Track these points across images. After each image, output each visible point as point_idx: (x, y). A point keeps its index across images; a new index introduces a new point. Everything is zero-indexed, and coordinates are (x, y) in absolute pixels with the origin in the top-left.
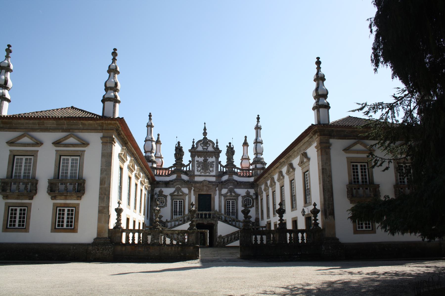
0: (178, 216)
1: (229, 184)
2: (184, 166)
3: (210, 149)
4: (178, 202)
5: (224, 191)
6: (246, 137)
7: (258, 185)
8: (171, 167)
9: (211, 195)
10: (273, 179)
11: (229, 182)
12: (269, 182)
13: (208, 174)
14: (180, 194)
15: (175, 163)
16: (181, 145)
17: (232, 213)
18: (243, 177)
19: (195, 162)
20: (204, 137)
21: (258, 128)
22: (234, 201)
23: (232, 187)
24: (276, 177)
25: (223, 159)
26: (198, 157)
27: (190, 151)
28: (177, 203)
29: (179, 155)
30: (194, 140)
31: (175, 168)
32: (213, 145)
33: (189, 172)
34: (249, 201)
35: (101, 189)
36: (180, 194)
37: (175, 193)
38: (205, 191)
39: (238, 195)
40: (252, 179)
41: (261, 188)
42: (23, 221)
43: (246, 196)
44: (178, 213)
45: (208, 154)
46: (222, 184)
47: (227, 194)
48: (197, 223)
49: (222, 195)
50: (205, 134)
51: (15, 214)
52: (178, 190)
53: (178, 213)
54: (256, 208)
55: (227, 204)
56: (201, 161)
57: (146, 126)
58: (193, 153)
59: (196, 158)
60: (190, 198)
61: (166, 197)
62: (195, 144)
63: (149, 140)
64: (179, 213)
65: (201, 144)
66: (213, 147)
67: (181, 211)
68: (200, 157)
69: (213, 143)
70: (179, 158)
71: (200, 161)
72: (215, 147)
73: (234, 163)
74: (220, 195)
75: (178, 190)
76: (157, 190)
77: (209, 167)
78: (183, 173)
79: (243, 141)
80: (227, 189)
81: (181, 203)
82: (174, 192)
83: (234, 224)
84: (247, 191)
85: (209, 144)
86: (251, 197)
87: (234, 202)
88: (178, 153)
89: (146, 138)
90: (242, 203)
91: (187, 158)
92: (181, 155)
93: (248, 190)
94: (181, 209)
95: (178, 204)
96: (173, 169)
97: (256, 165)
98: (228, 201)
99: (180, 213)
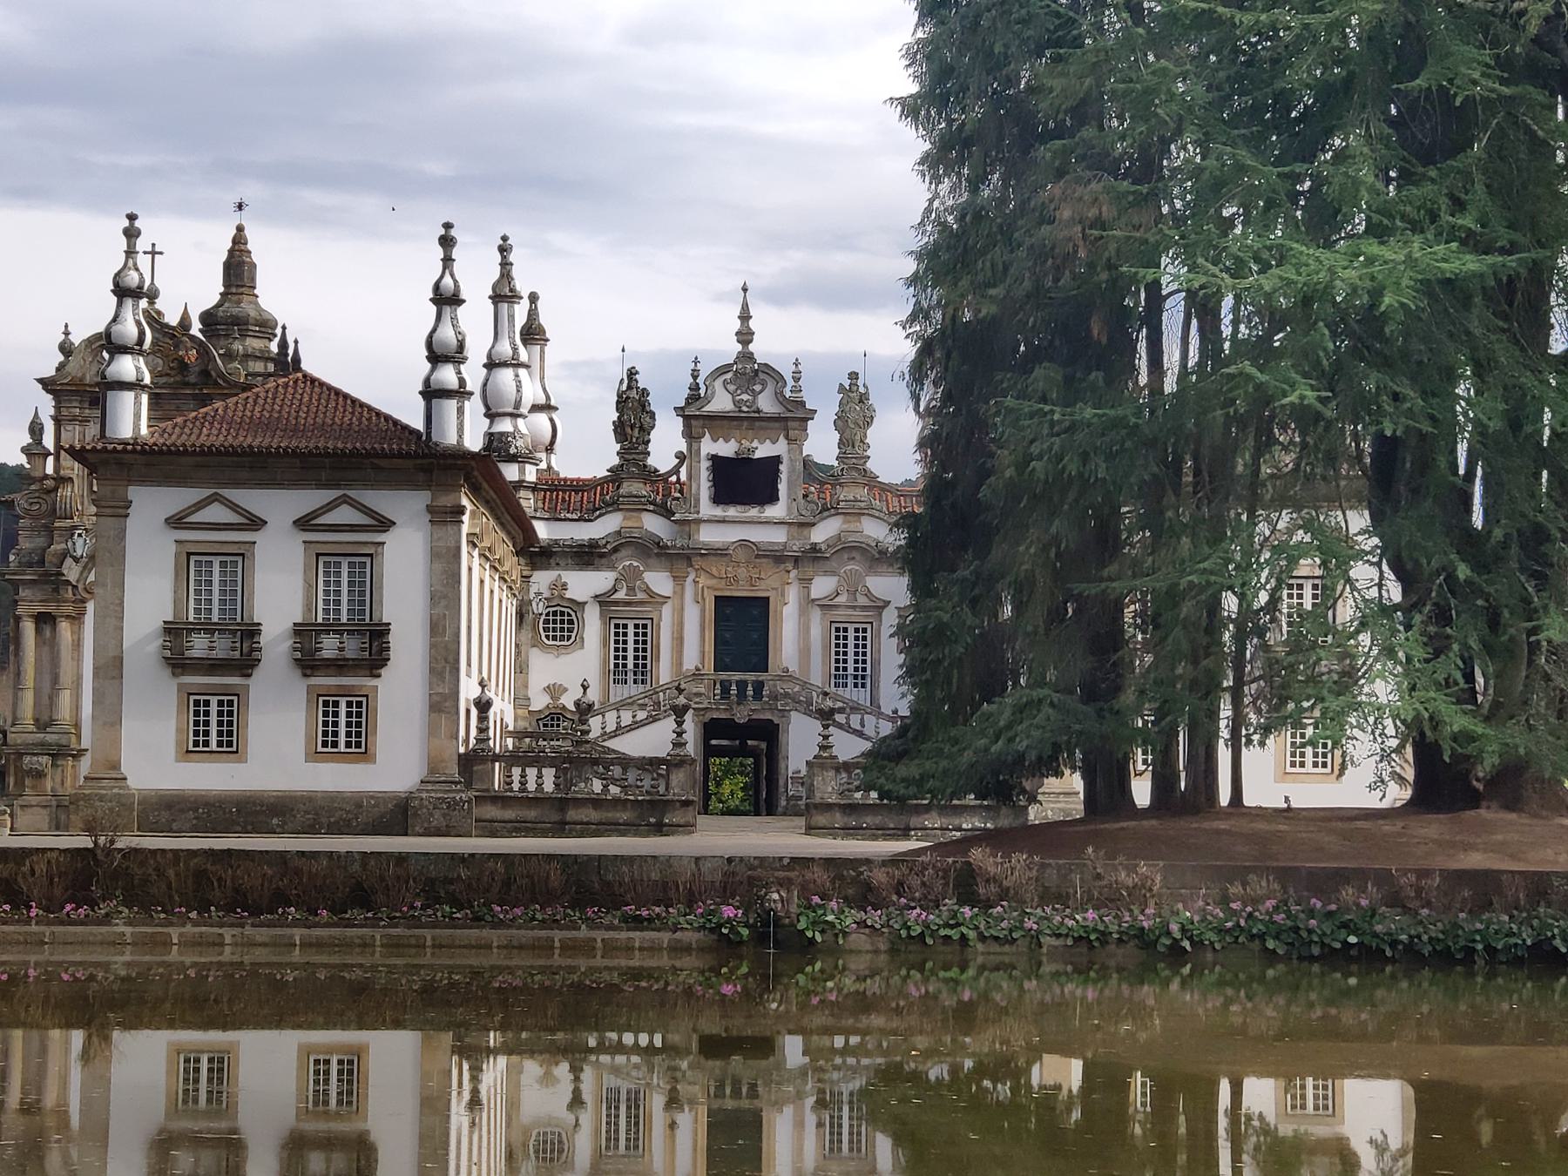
0: (632, 690)
3: (766, 404)
4: (631, 630)
5: (822, 586)
14: (641, 596)
15: (616, 461)
16: (641, 385)
17: (856, 677)
20: (739, 347)
25: (822, 444)
26: (715, 440)
30: (696, 362)
42: (230, 733)
44: (631, 677)
45: (757, 424)
46: (813, 557)
48: (709, 716)
49: (813, 600)
50: (745, 336)
51: (207, 713)
52: (630, 578)
53: (631, 677)
55: (834, 641)
57: (490, 297)
59: (708, 447)
60: (680, 612)
62: (700, 380)
63: (504, 364)
64: (635, 674)
66: (779, 396)
67: (645, 666)
69: (778, 378)
72: (788, 394)
73: (869, 465)
74: (808, 602)
75: (630, 578)
76: (542, 580)
78: (652, 508)
80: (835, 579)
81: (645, 634)
82: (615, 590)
83: (859, 728)
87: (865, 630)
89: (490, 350)
94: (645, 658)
95: (631, 638)
99: (642, 671)
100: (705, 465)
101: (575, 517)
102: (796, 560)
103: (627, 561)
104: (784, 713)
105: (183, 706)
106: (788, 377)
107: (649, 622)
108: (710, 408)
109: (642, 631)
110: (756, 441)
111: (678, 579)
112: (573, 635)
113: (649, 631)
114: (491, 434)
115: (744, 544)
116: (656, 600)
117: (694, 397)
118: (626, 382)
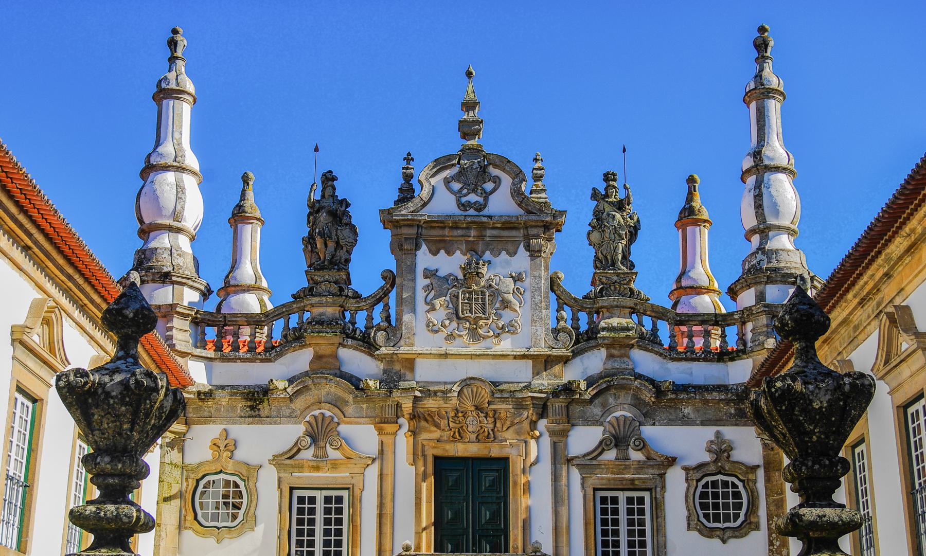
1: (611, 400)
4: (320, 506)
6: (691, 180)
8: (281, 312)
9: (505, 461)
11: (607, 389)
18: (686, 359)
19: (414, 280)
22: (643, 498)
23: (626, 417)
26: (435, 253)
27: (388, 219)
28: (312, 511)
29: (326, 245)
31: (307, 315)
32: (513, 184)
33: (379, 334)
34: (726, 495)
36: (333, 454)
37: (299, 450)
38: (474, 436)
43: (712, 468)
45: (489, 233)
47: (600, 454)
49: (569, 461)
54: (770, 535)
56: (450, 275)
58: (406, 231)
59: (424, 259)
61: (250, 472)
65: (447, 182)
66: (516, 193)
68: (442, 252)
69: (518, 175)
70: (328, 257)
71: (442, 273)
77: (498, 305)
78: (350, 341)
79: (682, 204)
81: (339, 511)
84: (713, 438)
85: (495, 182)
87: (641, 500)
88: (322, 234)
90: (689, 510)
92: (337, 243)
93: (718, 434)
95: (319, 517)
96: (294, 321)
97: (760, 287)
98: (609, 494)
101: (249, 355)
106: (529, 176)
107: (345, 494)
109: (334, 506)
110: (488, 253)
112: (241, 513)
113: (345, 505)
114: (145, 250)
118: (319, 187)
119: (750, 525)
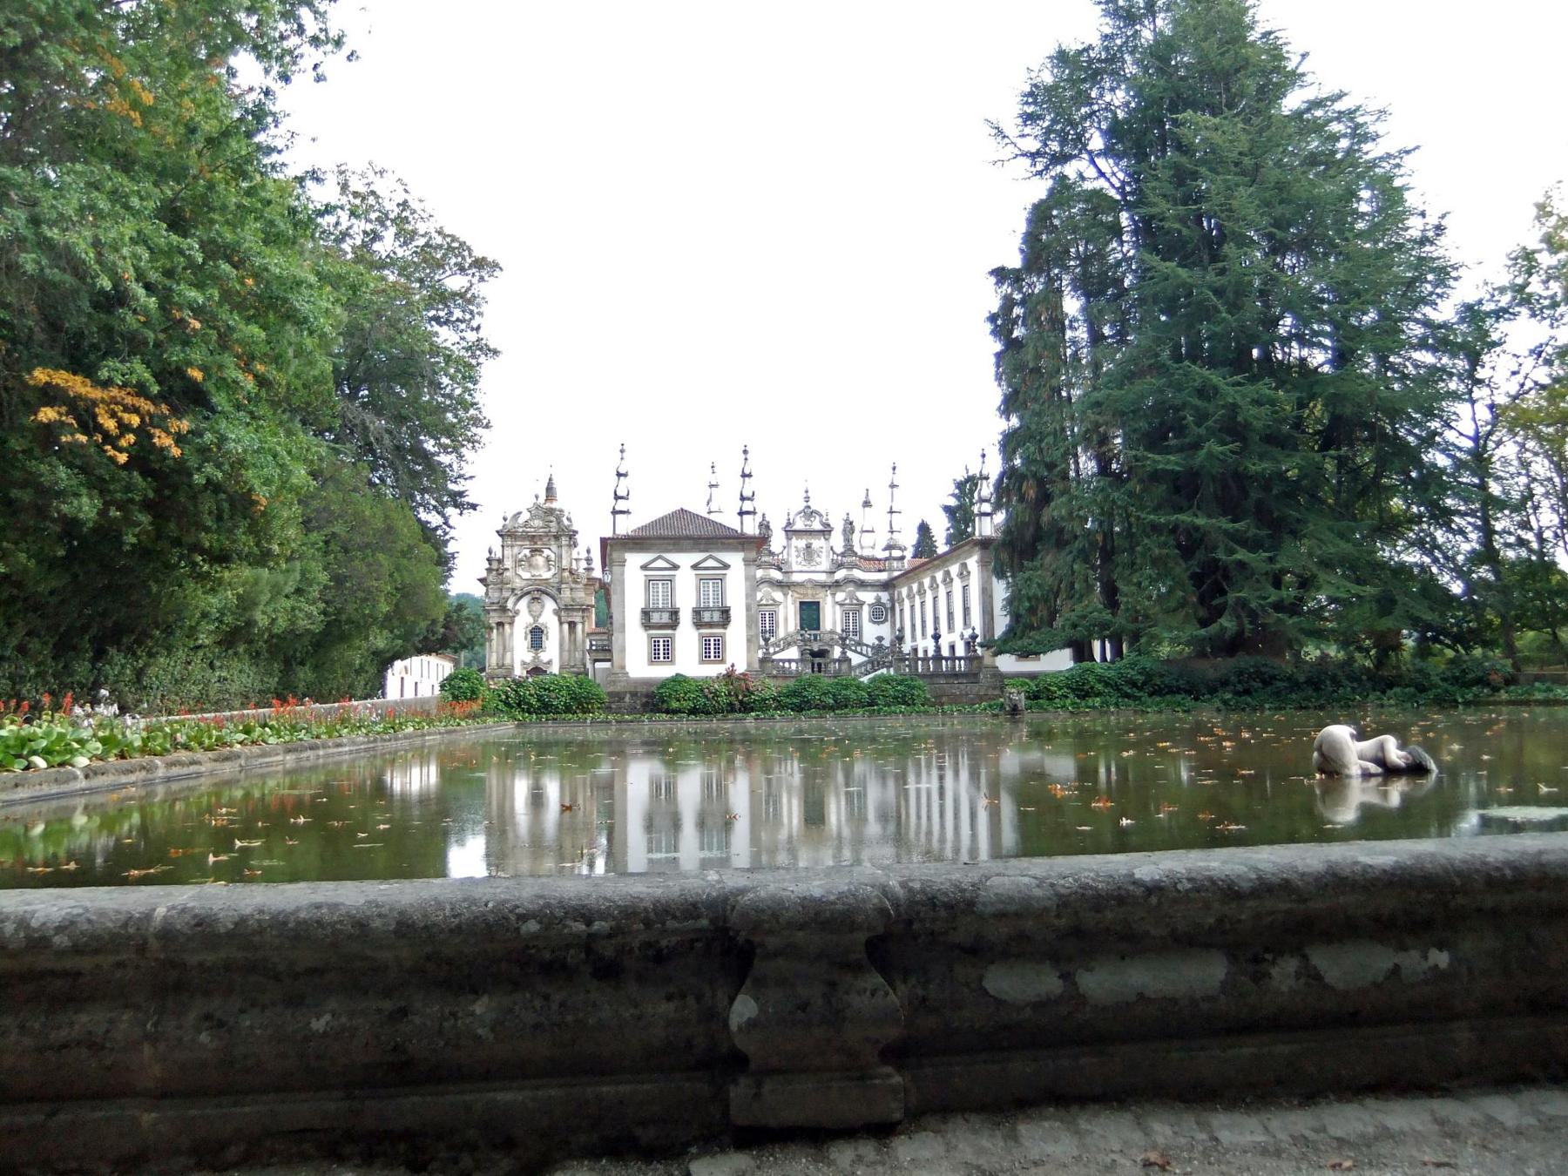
2: (771, 554)
3: (817, 526)
5: (840, 596)
7: (894, 587)
10: (921, 585)
12: (915, 587)
13: (813, 568)
21: (893, 486)
24: (927, 582)
25: (837, 541)
35: (748, 616)
39: (861, 604)
40: (884, 576)
41: (900, 593)
46: (837, 585)
50: (807, 499)
60: (786, 607)
62: (791, 518)
66: (821, 522)
69: (821, 515)
86: (883, 605)
91: (777, 542)
100: (793, 549)
102: (830, 587)
103: (765, 589)
104: (832, 646)
105: (649, 642)
108: (795, 528)
109: (771, 615)
111: (785, 595)
115: (810, 581)
116: (776, 603)
117: (789, 524)
119: (886, 620)
